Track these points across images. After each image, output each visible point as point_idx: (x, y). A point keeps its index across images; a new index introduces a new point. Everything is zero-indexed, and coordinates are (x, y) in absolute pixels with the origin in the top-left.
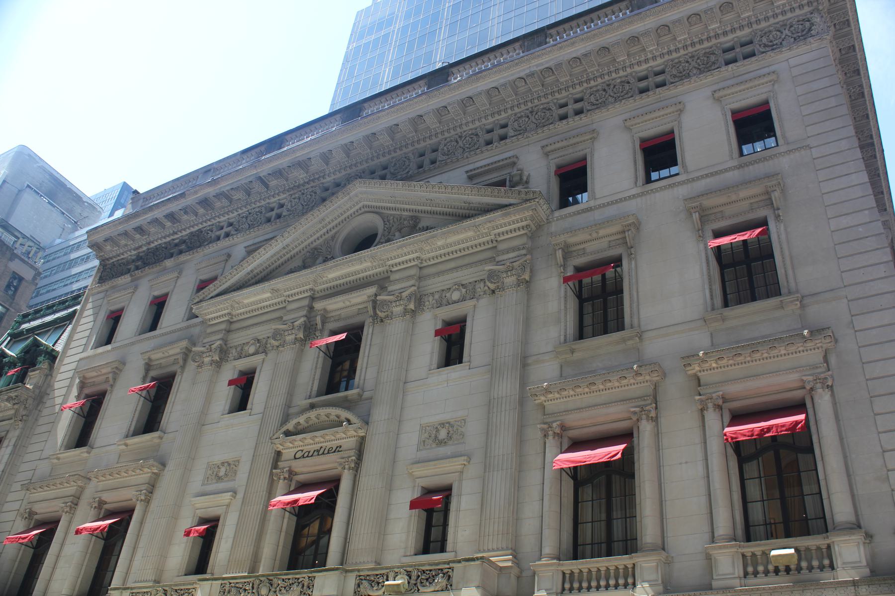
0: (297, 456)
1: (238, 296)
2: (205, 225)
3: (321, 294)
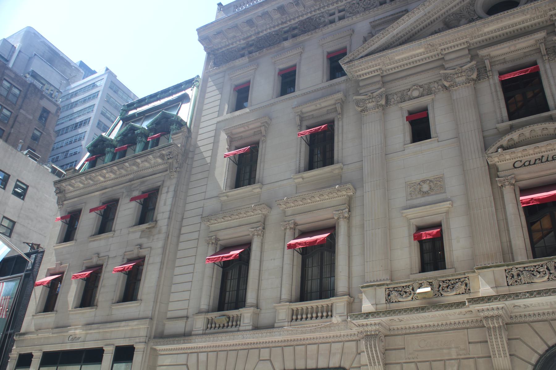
0: (516, 165)
1: (391, 53)
3: (476, 46)
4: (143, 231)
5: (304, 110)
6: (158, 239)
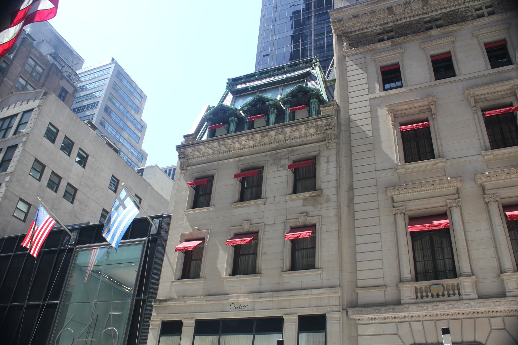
2: (457, 7)
4: (305, 199)
5: (477, 93)
6: (327, 207)
